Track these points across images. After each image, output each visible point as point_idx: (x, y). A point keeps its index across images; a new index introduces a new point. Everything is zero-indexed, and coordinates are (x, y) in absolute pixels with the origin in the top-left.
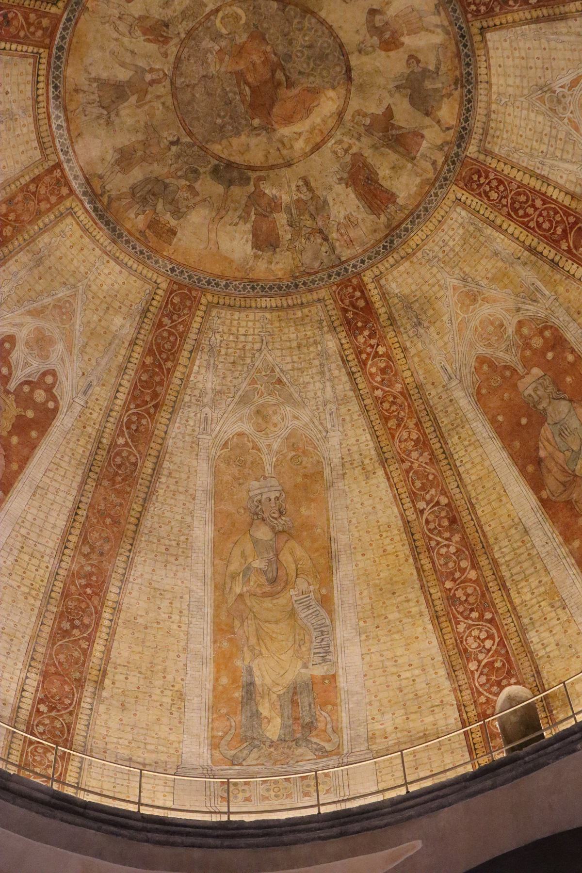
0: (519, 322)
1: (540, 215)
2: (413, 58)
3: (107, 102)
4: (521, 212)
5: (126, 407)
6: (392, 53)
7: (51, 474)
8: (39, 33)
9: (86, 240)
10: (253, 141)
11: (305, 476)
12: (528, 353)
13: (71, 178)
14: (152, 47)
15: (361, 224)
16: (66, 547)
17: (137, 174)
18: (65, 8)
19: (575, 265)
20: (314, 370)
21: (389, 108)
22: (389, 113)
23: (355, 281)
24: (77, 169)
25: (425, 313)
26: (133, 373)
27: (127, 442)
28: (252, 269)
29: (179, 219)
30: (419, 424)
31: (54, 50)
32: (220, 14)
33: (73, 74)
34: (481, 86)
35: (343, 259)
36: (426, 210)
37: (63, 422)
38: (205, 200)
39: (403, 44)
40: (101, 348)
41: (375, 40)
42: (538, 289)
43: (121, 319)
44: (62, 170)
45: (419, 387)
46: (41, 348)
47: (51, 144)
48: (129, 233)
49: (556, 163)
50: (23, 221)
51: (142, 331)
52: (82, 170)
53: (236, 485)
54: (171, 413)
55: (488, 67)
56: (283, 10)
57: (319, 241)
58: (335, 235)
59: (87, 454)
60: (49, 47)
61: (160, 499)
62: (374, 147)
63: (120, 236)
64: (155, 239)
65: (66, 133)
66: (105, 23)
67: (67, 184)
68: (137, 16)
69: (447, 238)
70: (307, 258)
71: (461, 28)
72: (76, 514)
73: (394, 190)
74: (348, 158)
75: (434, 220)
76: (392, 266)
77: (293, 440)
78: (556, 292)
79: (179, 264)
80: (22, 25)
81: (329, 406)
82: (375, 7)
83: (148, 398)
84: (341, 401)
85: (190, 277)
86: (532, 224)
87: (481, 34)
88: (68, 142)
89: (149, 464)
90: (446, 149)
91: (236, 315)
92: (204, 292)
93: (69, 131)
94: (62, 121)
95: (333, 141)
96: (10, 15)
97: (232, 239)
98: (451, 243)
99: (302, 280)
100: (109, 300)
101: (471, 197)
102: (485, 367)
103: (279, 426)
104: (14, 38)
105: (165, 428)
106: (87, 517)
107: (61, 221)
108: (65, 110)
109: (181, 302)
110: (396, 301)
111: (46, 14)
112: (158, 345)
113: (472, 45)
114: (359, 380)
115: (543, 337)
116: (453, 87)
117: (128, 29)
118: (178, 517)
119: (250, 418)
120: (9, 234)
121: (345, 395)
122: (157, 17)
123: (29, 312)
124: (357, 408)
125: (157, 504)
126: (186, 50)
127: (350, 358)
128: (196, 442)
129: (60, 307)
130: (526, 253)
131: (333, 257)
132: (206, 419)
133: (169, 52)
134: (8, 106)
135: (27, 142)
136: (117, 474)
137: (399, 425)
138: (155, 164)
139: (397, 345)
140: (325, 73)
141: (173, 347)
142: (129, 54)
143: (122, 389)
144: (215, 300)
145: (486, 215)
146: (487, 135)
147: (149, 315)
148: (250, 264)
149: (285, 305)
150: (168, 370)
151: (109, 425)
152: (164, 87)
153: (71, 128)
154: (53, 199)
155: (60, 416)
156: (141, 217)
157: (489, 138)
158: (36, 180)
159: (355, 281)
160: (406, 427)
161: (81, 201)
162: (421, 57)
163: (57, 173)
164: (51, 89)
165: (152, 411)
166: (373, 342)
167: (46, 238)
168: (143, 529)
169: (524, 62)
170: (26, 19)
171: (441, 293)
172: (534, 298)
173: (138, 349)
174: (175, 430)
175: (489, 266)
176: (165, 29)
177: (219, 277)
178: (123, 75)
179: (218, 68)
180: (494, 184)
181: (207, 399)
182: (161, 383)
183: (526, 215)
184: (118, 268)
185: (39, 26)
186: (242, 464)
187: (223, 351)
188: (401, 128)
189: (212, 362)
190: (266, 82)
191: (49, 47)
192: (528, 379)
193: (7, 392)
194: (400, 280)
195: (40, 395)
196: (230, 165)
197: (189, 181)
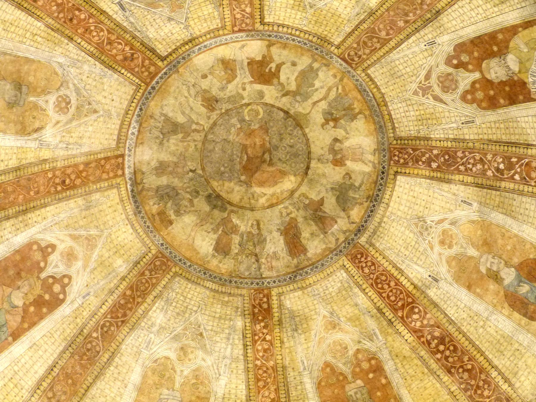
0: (358, 349)
1: (391, 291)
2: (348, 175)
3: (165, 131)
4: (380, 286)
5: (105, 315)
6: (337, 168)
7: (46, 339)
8: (146, 74)
9: (120, 207)
10: (237, 188)
11: (198, 397)
12: (358, 370)
13: (126, 166)
14: (203, 110)
15: (281, 260)
16: (38, 388)
17: (164, 180)
18: (167, 66)
19: (403, 327)
20: (224, 335)
21: (322, 199)
22: (321, 202)
23: (266, 292)
24: (132, 162)
25: (302, 325)
26: (116, 297)
27: (98, 337)
28: (208, 262)
29: (177, 216)
30: (277, 390)
31: (149, 88)
32: (249, 107)
33: (154, 106)
34: (382, 205)
35: (264, 276)
36: (323, 265)
37: (65, 310)
38: (196, 211)
39: (345, 165)
40: (103, 274)
41: (331, 157)
42: (375, 333)
43: (121, 262)
44: (124, 160)
45: (284, 368)
46: (69, 260)
47: (124, 141)
48: (146, 213)
49: (412, 264)
50: (89, 180)
51: (131, 274)
52: (134, 164)
53: (154, 388)
54: (130, 329)
55: (391, 196)
56: (286, 120)
57: (253, 260)
58: (263, 260)
59: (72, 335)
60: (147, 84)
61: (106, 379)
62: (305, 218)
63: (140, 212)
64: (159, 222)
65: (135, 138)
67: (123, 169)
68: (203, 88)
69: (329, 286)
70: (242, 268)
71: (384, 168)
72: (52, 370)
73: (308, 247)
74: (288, 219)
75: (325, 273)
76: (291, 290)
77: (197, 373)
78: (386, 339)
79: (167, 243)
80: (139, 65)
81: (225, 360)
82: (339, 138)
83: (120, 315)
84: (235, 360)
85: (171, 253)
86: (384, 295)
87: (394, 175)
88: (134, 145)
89: (107, 356)
90: (347, 234)
91: (190, 285)
92: (176, 265)
93: (137, 138)
94: (135, 131)
95: (282, 206)
96: (135, 56)
97: (203, 240)
98: (331, 290)
99: (235, 279)
100: (119, 247)
101: (352, 267)
102: (328, 370)
103: (192, 361)
104: (131, 70)
105: (123, 337)
106: (58, 374)
107: (110, 189)
108: (141, 125)
109: (160, 265)
110: (287, 312)
111: (155, 65)
112: (137, 285)
113: (387, 179)
114: (249, 351)
115: (370, 364)
116: (365, 200)
118: (113, 395)
119: (176, 350)
120: (78, 184)
121: (238, 357)
122: (214, 93)
123: (70, 235)
124: (242, 367)
125: (103, 382)
127: (248, 336)
128: (139, 353)
129: (89, 240)
130: (375, 311)
131: (258, 273)
132: (150, 342)
134: (110, 108)
135: (111, 134)
136: (85, 354)
137: (264, 387)
138: (177, 179)
139: (279, 338)
140: (293, 165)
141: (146, 290)
142: (189, 109)
143: (106, 304)
144: (180, 272)
145: (358, 280)
146: (375, 234)
147: (139, 266)
148: (209, 258)
149: (220, 290)
150: (138, 303)
151: (91, 322)
153: (140, 137)
154: (111, 174)
155: (64, 306)
156: (156, 206)
157: (376, 236)
158: (107, 159)
159: (266, 292)
160: (269, 389)
161: (126, 182)
162: (353, 176)
163: (120, 160)
164: (138, 110)
165: (120, 324)
166: (265, 331)
167: (96, 196)
168: (89, 395)
169: (414, 200)
170: (143, 62)
171: (315, 317)
172: (371, 338)
173: (125, 283)
174: (129, 340)
175: (350, 311)
177: (187, 259)
178: (181, 119)
180: (369, 264)
181: (155, 329)
182: (130, 309)
183: (382, 288)
184: (131, 231)
185: (147, 70)
186: (162, 376)
187: (174, 304)
188: (325, 212)
189: (165, 308)
190: (257, 157)
191: (147, 84)
192: (353, 385)
193: (38, 278)
194: (293, 300)
195: (57, 288)
196: (218, 196)
197: (192, 196)
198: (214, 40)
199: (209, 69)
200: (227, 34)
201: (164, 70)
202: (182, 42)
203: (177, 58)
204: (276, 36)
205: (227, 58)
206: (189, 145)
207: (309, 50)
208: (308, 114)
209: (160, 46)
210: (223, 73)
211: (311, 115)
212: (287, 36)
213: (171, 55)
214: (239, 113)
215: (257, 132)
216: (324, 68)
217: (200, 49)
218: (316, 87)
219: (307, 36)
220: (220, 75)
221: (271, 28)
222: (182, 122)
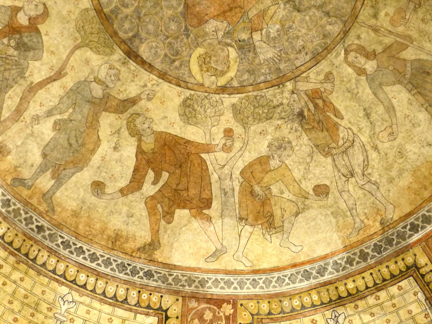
18: (408, 248)
32: (222, 81)
66: (375, 183)
68: (329, 160)
117: (351, 151)
122: (305, 138)
126: (298, 63)
133: (322, 77)
142: (374, 116)
152: (359, 37)
176: (306, 113)
179: (273, 9)
198: (284, 289)
199: (306, 208)
200: (250, 298)
201: (416, 237)
202: (361, 304)
203: (380, 263)
204: (134, 272)
205: (258, 230)
206: (392, 22)
207: (59, 226)
208: (77, 47)
209: (415, 309)
210: (275, 190)
211: (70, 44)
212: (108, 271)
213: (393, 276)
214: (251, 72)
215: (212, 11)
216: (26, 174)
217: (321, 272)
218: (50, 122)
219: (61, 267)
220: (280, 185)
221: (145, 296)
222: (398, 87)
